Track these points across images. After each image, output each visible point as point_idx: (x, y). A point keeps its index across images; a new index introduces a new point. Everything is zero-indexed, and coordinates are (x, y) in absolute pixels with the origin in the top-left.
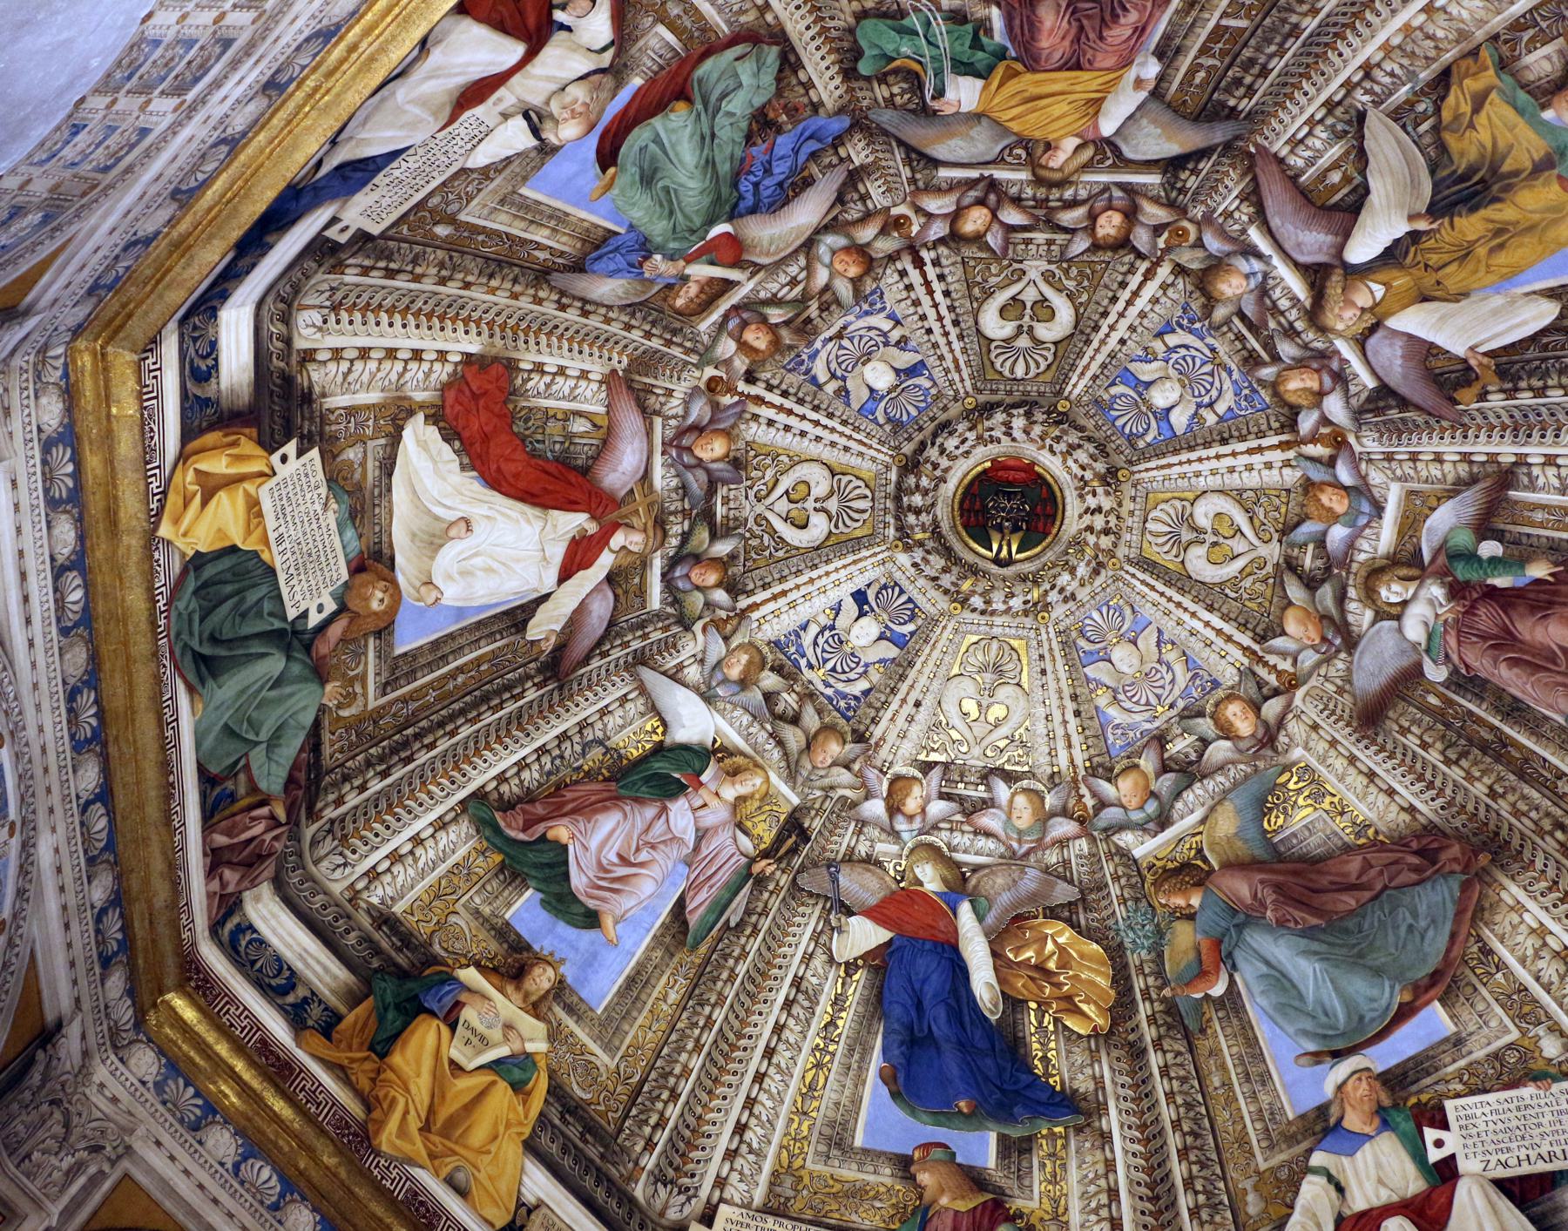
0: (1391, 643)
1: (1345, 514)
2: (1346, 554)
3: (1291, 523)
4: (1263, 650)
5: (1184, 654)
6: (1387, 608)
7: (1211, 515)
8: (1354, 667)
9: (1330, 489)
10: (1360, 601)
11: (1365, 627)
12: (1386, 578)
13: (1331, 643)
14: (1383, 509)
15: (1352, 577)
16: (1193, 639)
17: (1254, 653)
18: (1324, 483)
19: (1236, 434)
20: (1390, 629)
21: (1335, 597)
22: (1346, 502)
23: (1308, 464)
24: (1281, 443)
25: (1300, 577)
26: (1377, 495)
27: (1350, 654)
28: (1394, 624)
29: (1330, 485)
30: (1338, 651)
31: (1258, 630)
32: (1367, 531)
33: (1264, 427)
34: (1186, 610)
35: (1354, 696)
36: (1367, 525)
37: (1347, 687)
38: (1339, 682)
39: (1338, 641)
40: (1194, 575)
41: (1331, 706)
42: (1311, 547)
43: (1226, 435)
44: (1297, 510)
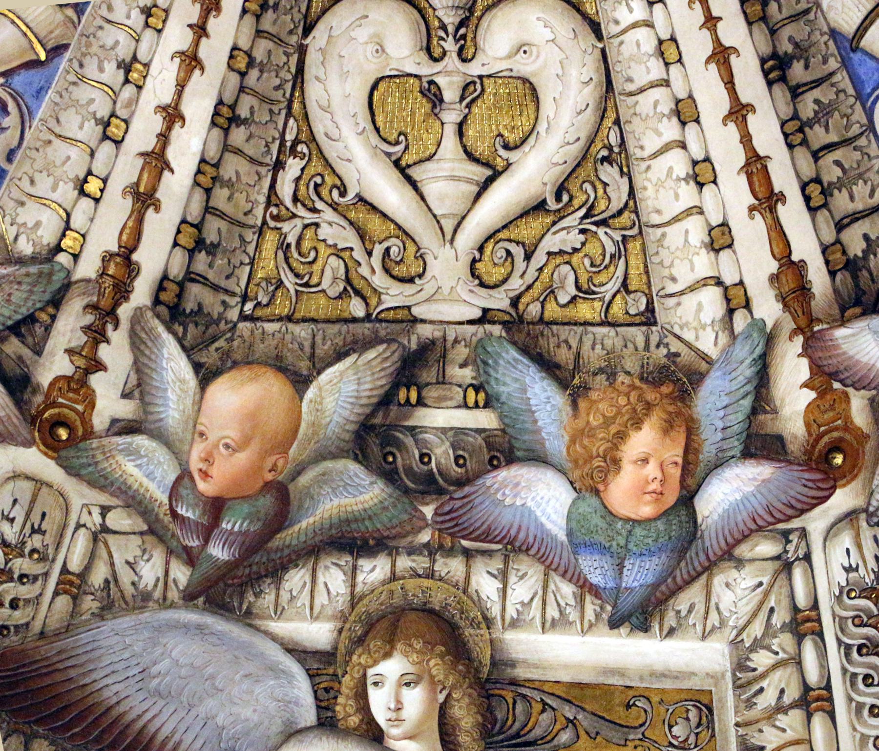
0: (247, 712)
1: (609, 514)
2: (486, 537)
3: (548, 344)
4: (137, 318)
5: (57, 51)
6: (348, 682)
7: (524, 66)
8: (152, 616)
9: (675, 452)
10: (354, 600)
11: (278, 627)
12: (436, 666)
13: (207, 532)
14: (644, 628)
15: (421, 563)
16: (112, 74)
17: (122, 291)
18: (691, 430)
19: (807, 108)
20: (289, 703)
21: (348, 521)
22: (647, 510)
23: (746, 371)
24: (798, 269)
25: (386, 400)
26: (682, 602)
27: (189, 597)
28: (308, 715)
29: (690, 450)
30: (190, 558)
31: (195, 291)
32: (567, 590)
33: (842, 203)
34: (200, 30)
35: (68, 629)
36: (585, 587)
37: (89, 604)
38: (98, 576)
39: (218, 552)
40: (319, 35)
41: (20, 565)
42: (486, 419)
43: (798, 72)
44: (594, 357)
